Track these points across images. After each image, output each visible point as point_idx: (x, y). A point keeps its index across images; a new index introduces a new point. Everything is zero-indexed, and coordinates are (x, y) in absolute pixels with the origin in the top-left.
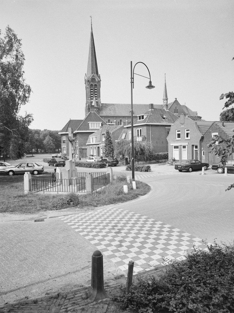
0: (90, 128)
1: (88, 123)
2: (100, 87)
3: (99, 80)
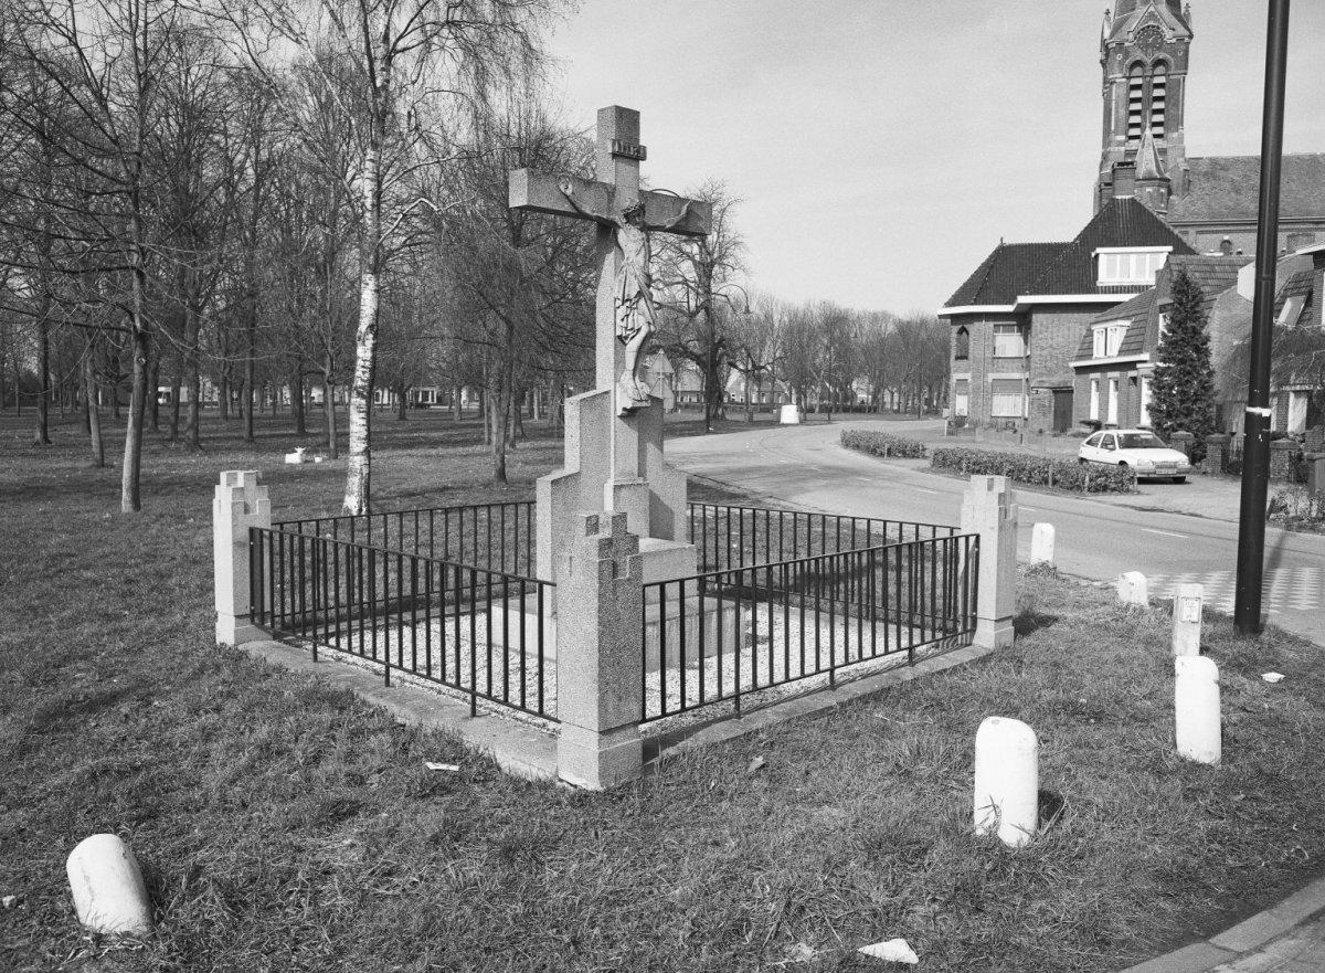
0: (1105, 277)
1: (1093, 255)
2: (1186, 68)
3: (1181, 30)
